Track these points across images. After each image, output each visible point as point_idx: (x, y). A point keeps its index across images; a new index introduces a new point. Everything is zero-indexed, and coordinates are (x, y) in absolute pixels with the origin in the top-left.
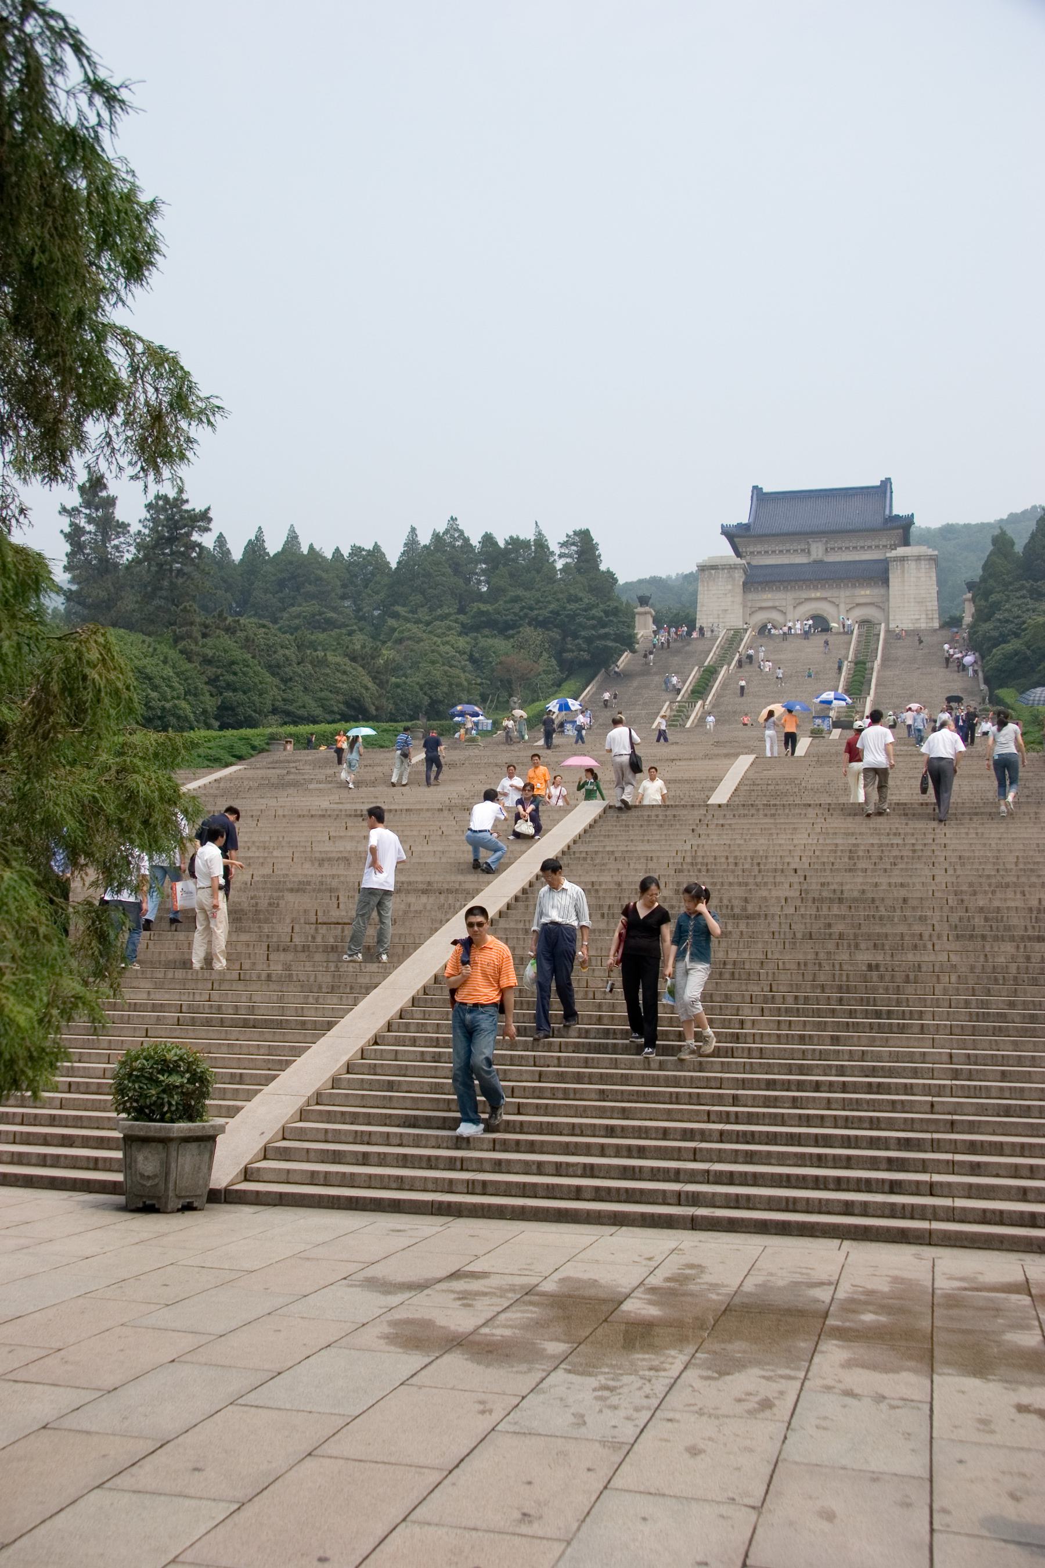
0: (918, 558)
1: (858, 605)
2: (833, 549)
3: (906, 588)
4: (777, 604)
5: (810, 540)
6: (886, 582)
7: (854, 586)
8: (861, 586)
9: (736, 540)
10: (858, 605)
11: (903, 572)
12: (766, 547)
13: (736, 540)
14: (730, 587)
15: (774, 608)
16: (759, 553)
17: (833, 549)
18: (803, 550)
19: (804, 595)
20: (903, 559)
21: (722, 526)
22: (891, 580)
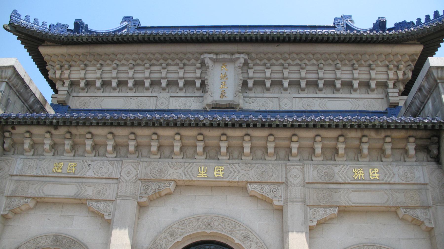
2: (260, 83)
4: (89, 192)
9: (43, 50)
10: (344, 212)
12: (110, 73)
13: (43, 50)
15: (80, 203)
16: (89, 84)
17: (260, 83)
18: (189, 83)
19: (175, 170)
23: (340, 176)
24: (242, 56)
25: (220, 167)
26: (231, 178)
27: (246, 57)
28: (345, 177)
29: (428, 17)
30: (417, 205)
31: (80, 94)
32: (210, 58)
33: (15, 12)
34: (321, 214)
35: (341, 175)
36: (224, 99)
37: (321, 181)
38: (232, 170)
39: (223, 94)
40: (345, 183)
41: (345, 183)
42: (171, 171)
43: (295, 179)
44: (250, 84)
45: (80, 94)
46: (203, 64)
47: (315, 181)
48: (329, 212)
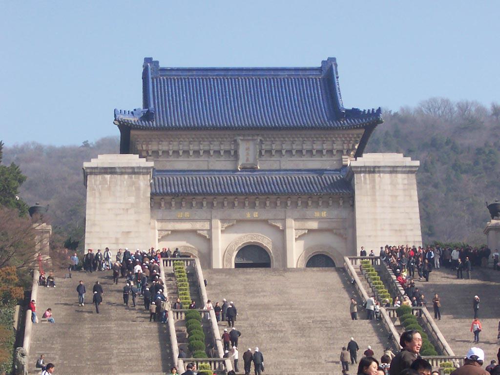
0: (393, 170)
5: (239, 139)
6: (349, 200)
7: (306, 205)
8: (317, 205)
11: (374, 188)
14: (132, 199)
19: (236, 214)
20: (372, 170)
29: (369, 110)
36: (248, 162)
39: (247, 160)
44: (263, 152)
46: (235, 141)
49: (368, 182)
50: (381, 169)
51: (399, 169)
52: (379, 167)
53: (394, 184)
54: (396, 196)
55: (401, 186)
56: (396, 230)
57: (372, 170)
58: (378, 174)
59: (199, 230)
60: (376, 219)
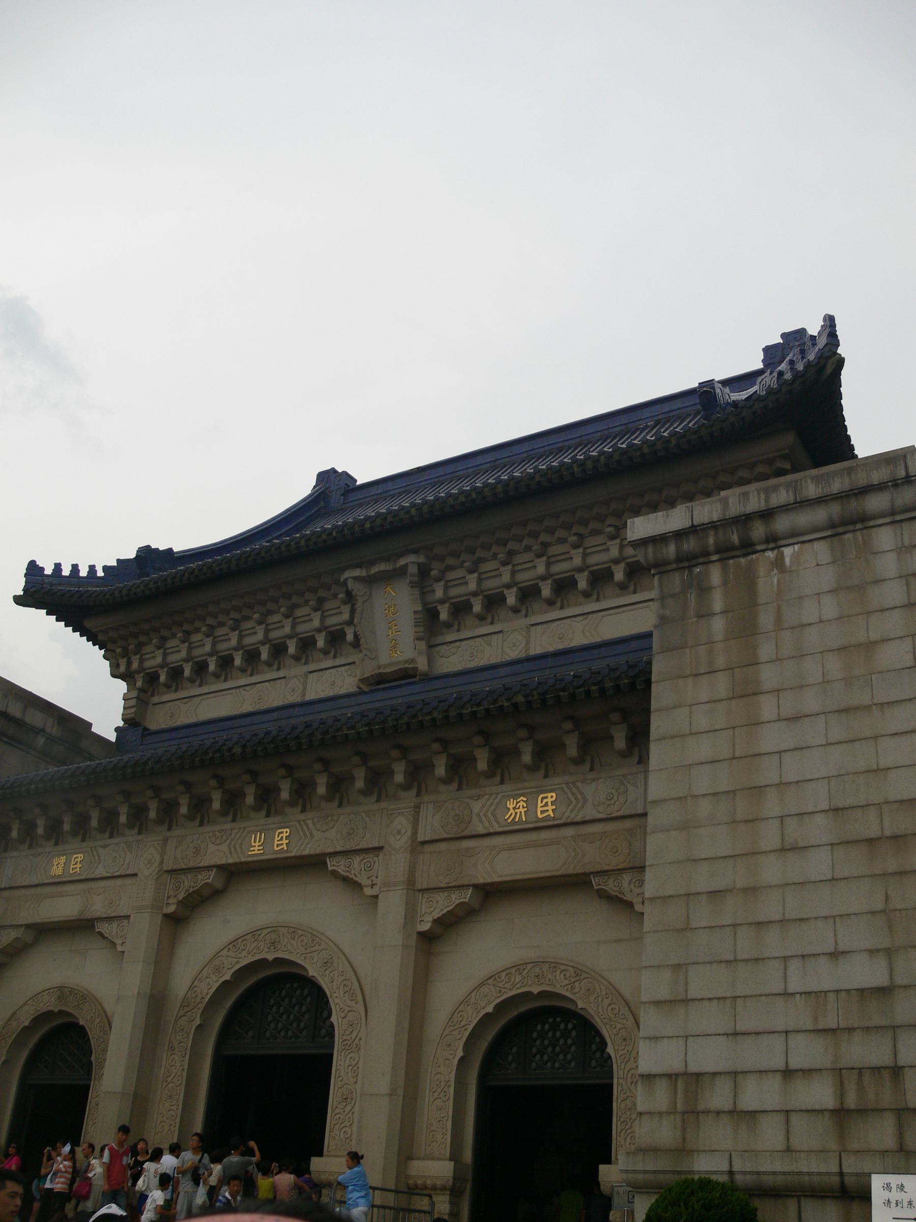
1: (492, 894)
2: (461, 609)
3: (771, 738)
7: (460, 771)
9: (88, 624)
11: (745, 629)
17: (461, 609)
21: (33, 569)
22: (661, 694)
23: (481, 821)
24: (411, 558)
25: (284, 830)
26: (298, 851)
27: (422, 559)
28: (489, 822)
30: (621, 866)
31: (165, 698)
32: (356, 579)
33: (32, 565)
34: (441, 905)
35: (483, 818)
37: (446, 836)
38: (301, 833)
40: (489, 835)
41: (489, 835)
42: (212, 848)
43: (398, 837)
44: (444, 615)
45: (165, 698)
47: (435, 837)
48: (456, 898)
49: (718, 603)
50: (782, 524)
51: (876, 503)
52: (767, 515)
53: (854, 589)
54: (870, 646)
55: (894, 593)
56: (870, 841)
57: (735, 539)
58: (770, 554)
59: (100, 919)
60: (757, 791)
